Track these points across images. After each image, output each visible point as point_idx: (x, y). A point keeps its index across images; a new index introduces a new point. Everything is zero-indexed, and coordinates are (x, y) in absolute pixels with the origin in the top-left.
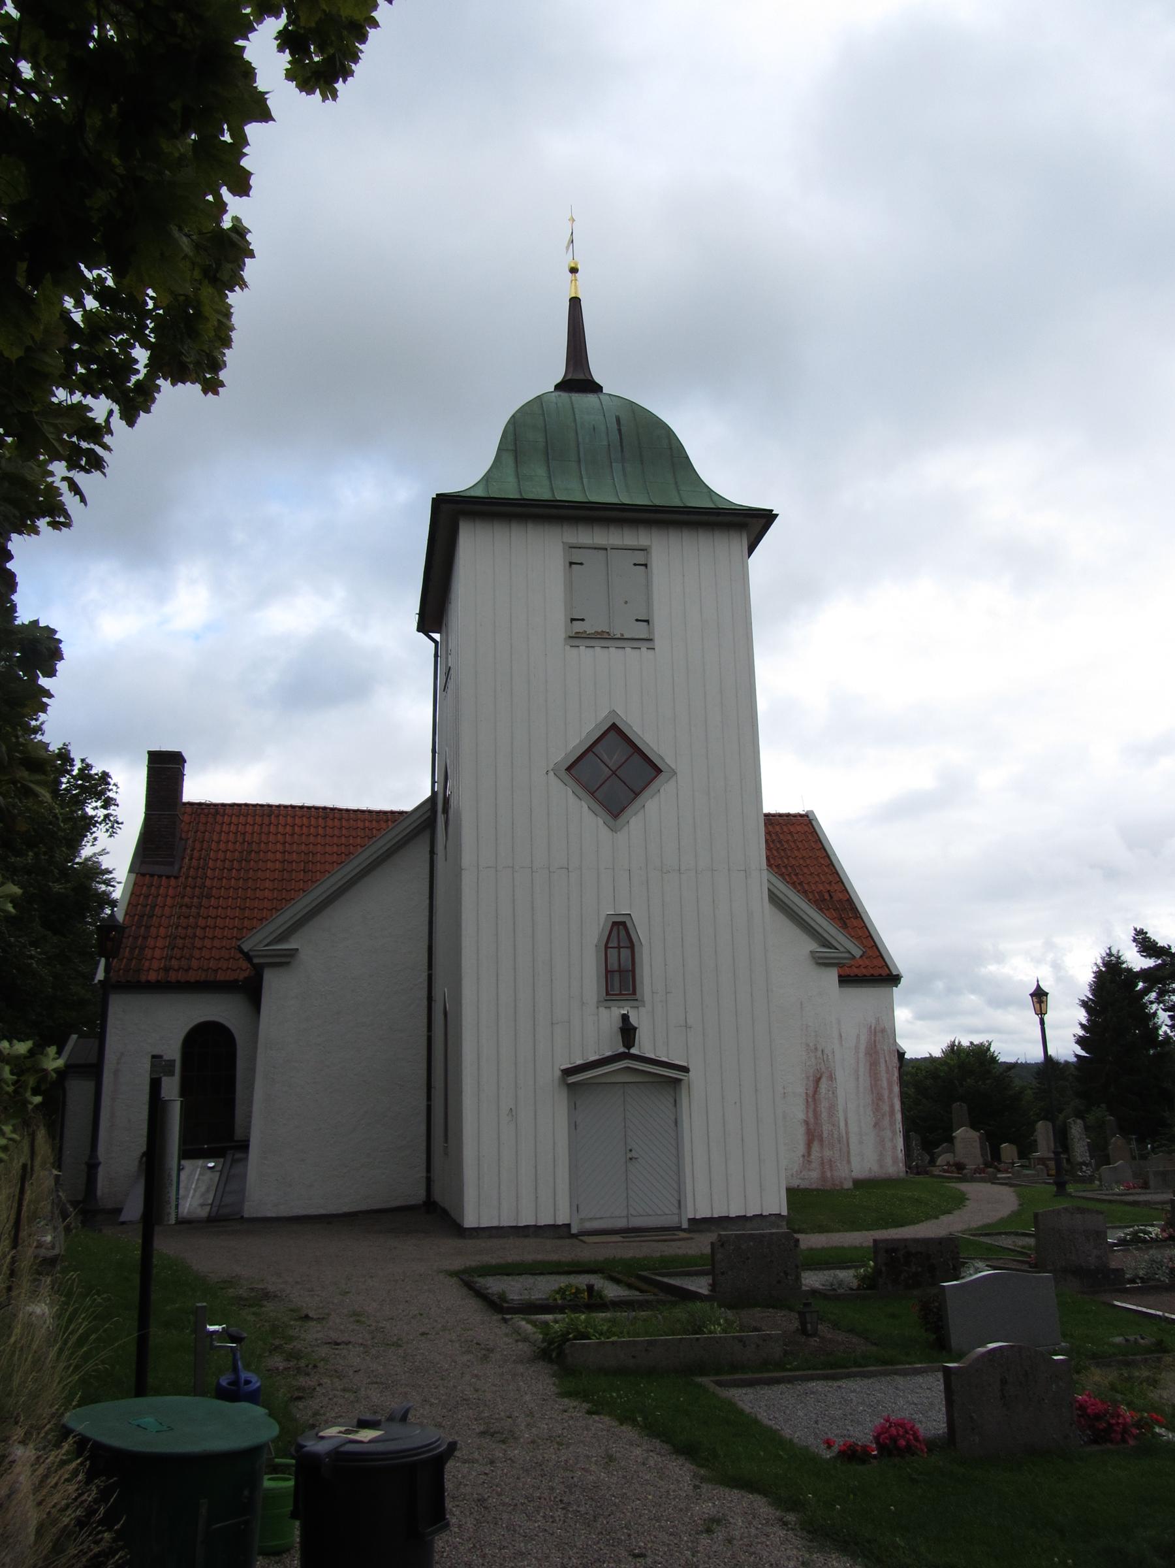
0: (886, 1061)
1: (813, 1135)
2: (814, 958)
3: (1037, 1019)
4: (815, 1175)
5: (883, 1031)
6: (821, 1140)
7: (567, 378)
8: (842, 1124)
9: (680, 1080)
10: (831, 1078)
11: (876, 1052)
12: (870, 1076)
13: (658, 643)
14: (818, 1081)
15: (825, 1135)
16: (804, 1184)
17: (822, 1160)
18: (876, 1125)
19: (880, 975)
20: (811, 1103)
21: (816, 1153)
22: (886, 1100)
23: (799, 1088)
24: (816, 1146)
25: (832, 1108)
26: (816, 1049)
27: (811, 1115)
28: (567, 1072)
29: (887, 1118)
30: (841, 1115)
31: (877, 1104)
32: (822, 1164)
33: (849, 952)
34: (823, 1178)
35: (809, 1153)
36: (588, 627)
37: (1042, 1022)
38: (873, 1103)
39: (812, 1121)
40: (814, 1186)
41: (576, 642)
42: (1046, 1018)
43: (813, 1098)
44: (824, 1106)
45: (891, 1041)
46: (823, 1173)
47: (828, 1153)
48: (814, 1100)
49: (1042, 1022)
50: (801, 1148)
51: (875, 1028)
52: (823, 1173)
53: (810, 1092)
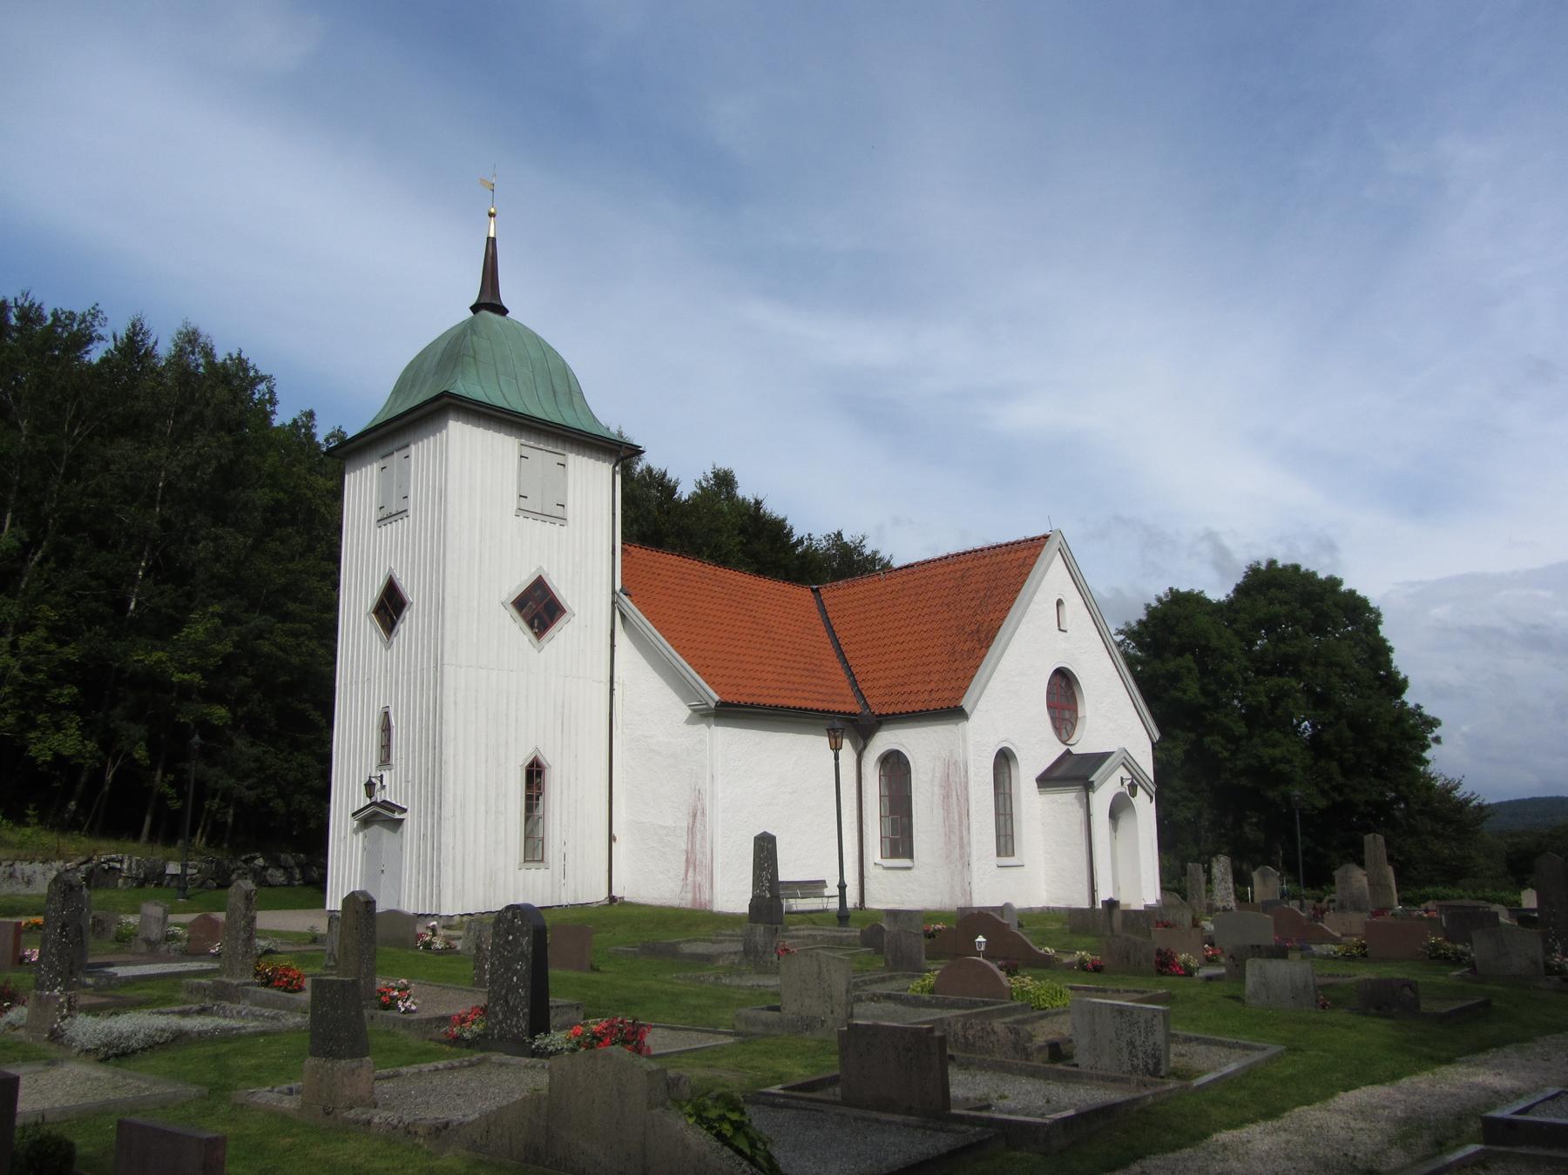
0: (957, 795)
1: (690, 862)
2: (694, 711)
3: (832, 754)
4: (690, 896)
5: (955, 763)
6: (695, 868)
7: (482, 301)
8: (709, 853)
9: (402, 820)
10: (703, 813)
11: (949, 785)
12: (943, 809)
13: (411, 512)
14: (695, 816)
15: (697, 863)
16: (683, 904)
17: (695, 882)
18: (947, 858)
19: (942, 708)
20: (690, 836)
21: (690, 879)
22: (957, 832)
23: (684, 823)
24: (691, 873)
25: (703, 838)
26: (695, 790)
27: (690, 846)
28: (353, 815)
29: (957, 851)
30: (708, 846)
31: (950, 838)
32: (694, 887)
33: (707, 704)
34: (694, 899)
35: (687, 879)
36: (385, 513)
37: (837, 758)
38: (945, 835)
39: (690, 850)
40: (689, 906)
41: (383, 522)
42: (840, 752)
43: (692, 830)
44: (699, 836)
45: (963, 773)
46: (695, 894)
47: (699, 878)
48: (692, 833)
49: (837, 758)
50: (683, 872)
51: (949, 761)
52: (695, 894)
53: (690, 826)
